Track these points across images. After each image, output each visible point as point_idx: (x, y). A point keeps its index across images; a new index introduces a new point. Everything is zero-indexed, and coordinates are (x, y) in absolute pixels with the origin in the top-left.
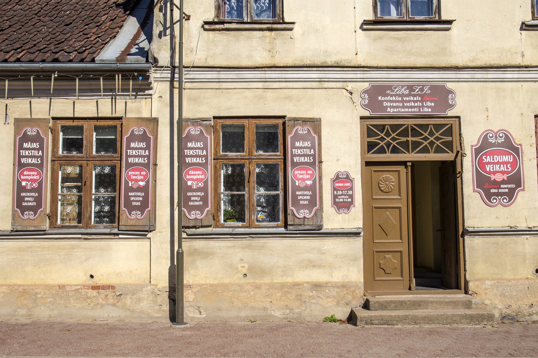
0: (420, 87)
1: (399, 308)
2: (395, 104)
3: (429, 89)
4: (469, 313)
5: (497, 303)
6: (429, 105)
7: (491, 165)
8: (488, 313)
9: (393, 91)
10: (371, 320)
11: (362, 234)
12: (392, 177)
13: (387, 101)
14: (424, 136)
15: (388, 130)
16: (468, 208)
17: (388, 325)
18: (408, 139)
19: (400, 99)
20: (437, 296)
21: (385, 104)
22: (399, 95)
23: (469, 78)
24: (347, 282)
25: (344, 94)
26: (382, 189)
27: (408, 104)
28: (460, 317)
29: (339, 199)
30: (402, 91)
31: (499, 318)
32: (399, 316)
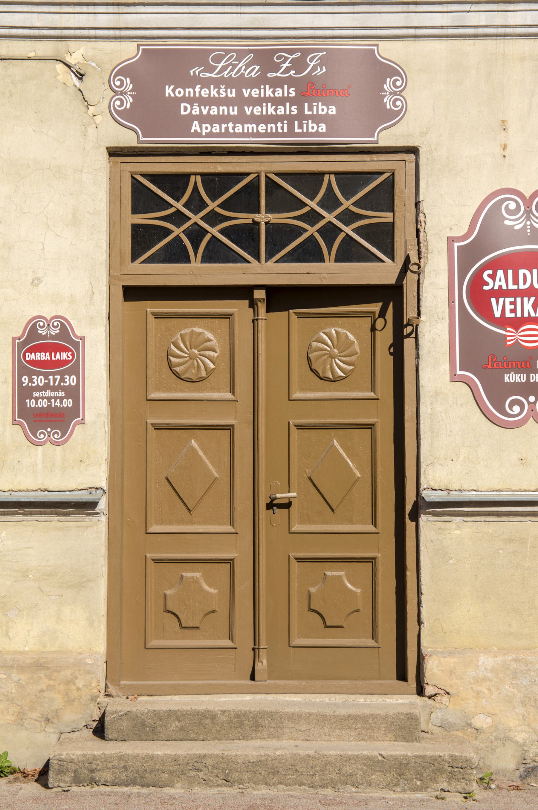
0: (294, 56)
1: (193, 735)
2: (214, 111)
3: (323, 62)
4: (394, 753)
5: (512, 724)
6: (320, 112)
7: (508, 300)
8: (451, 756)
9: (211, 69)
10: (92, 771)
11: (102, 505)
12: (209, 335)
13: (191, 101)
14: (306, 210)
15: (195, 188)
16: (433, 431)
17: (143, 786)
18: (257, 217)
19: (232, 94)
20: (326, 698)
21: (185, 109)
22: (229, 83)
23: (447, 27)
24: (53, 652)
25: (60, 78)
26: (178, 369)
27: (257, 111)
28: (365, 765)
29: (37, 399)
30: (240, 69)
31: (518, 773)
32: (176, 760)
